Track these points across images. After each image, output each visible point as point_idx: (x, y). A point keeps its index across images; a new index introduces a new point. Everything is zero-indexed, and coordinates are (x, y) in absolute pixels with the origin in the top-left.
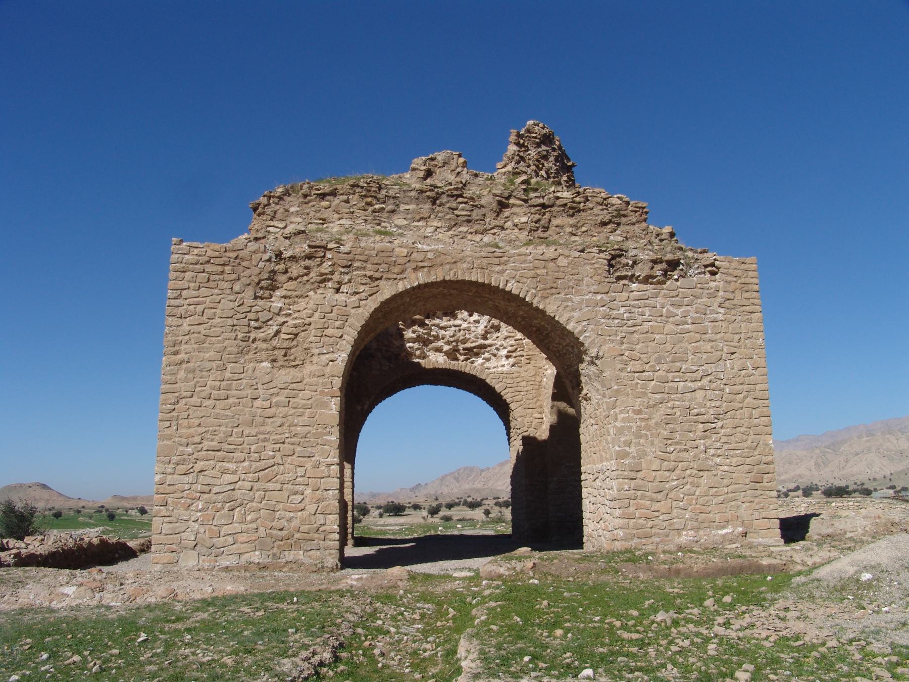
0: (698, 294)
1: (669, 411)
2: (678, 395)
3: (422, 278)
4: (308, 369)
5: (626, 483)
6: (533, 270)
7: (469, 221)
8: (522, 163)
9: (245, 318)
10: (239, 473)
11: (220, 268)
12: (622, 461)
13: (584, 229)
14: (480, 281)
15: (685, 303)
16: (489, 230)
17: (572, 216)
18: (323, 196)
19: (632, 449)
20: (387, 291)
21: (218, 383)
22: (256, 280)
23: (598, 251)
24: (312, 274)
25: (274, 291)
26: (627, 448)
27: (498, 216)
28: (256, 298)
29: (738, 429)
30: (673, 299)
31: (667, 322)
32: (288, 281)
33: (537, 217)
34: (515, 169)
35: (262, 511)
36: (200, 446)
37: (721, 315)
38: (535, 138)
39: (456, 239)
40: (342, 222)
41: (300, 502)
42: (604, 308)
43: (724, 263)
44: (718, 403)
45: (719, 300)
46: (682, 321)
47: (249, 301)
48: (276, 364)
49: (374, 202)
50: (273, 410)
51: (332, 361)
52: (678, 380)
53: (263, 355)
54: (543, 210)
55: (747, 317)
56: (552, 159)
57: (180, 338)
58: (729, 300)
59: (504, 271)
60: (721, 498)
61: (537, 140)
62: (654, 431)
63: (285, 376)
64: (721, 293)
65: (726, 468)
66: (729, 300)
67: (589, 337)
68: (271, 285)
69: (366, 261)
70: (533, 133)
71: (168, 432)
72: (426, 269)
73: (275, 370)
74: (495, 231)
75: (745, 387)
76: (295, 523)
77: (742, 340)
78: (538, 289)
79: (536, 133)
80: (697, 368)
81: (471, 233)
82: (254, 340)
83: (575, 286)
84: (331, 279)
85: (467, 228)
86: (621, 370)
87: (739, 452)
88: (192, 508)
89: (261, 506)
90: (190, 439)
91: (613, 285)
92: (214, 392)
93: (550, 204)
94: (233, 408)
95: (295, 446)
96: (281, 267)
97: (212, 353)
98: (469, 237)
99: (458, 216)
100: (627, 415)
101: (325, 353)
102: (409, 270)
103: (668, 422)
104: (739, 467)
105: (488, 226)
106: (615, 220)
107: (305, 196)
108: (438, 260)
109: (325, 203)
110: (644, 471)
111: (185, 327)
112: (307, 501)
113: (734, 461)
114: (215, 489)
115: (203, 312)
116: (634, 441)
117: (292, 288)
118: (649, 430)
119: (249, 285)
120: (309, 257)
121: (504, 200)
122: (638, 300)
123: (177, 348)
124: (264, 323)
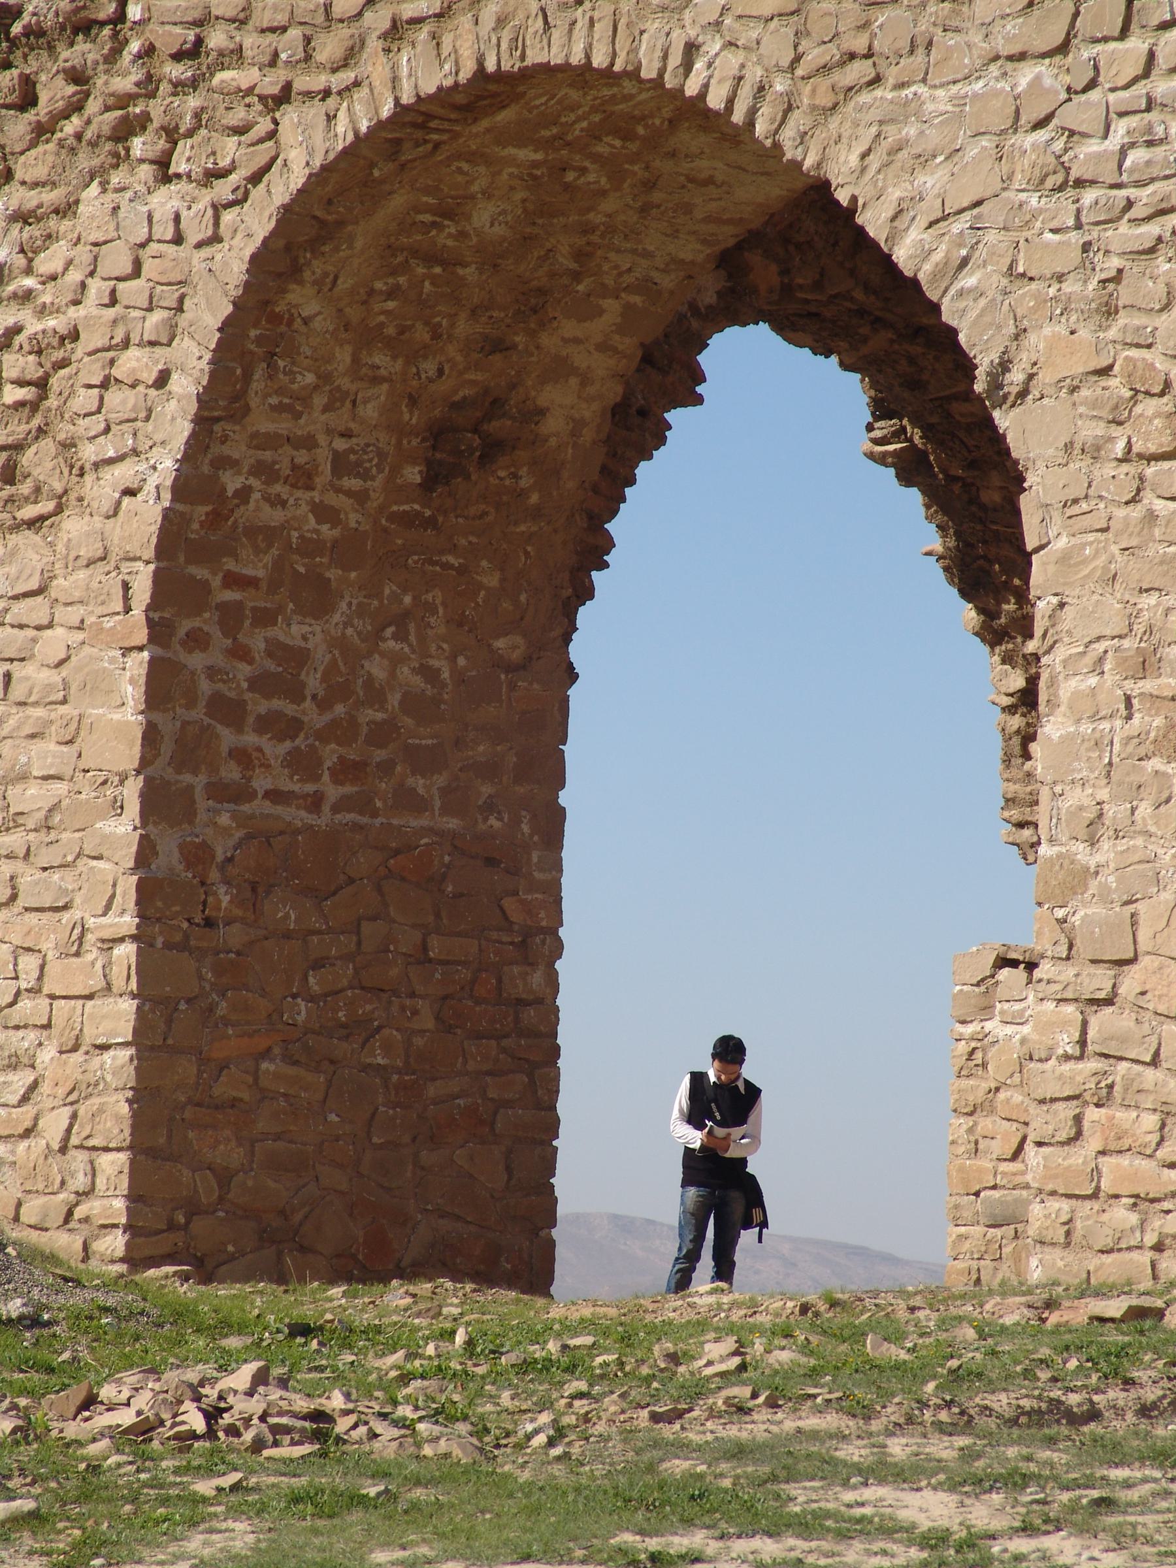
4: (73, 526)
5: (1064, 1024)
12: (1060, 913)
14: (599, 60)
19: (1107, 851)
24: (93, 106)
32: (33, 144)
41: (25, 1099)
42: (1042, 135)
51: (130, 492)
67: (978, 293)
72: (423, 34)
78: (799, 72)
86: (1095, 451)
95: (18, 866)
100: (1093, 681)
101: (111, 461)
102: (374, 44)
110: (1145, 961)
112: (45, 1088)
116: (1110, 811)
117: (40, 172)
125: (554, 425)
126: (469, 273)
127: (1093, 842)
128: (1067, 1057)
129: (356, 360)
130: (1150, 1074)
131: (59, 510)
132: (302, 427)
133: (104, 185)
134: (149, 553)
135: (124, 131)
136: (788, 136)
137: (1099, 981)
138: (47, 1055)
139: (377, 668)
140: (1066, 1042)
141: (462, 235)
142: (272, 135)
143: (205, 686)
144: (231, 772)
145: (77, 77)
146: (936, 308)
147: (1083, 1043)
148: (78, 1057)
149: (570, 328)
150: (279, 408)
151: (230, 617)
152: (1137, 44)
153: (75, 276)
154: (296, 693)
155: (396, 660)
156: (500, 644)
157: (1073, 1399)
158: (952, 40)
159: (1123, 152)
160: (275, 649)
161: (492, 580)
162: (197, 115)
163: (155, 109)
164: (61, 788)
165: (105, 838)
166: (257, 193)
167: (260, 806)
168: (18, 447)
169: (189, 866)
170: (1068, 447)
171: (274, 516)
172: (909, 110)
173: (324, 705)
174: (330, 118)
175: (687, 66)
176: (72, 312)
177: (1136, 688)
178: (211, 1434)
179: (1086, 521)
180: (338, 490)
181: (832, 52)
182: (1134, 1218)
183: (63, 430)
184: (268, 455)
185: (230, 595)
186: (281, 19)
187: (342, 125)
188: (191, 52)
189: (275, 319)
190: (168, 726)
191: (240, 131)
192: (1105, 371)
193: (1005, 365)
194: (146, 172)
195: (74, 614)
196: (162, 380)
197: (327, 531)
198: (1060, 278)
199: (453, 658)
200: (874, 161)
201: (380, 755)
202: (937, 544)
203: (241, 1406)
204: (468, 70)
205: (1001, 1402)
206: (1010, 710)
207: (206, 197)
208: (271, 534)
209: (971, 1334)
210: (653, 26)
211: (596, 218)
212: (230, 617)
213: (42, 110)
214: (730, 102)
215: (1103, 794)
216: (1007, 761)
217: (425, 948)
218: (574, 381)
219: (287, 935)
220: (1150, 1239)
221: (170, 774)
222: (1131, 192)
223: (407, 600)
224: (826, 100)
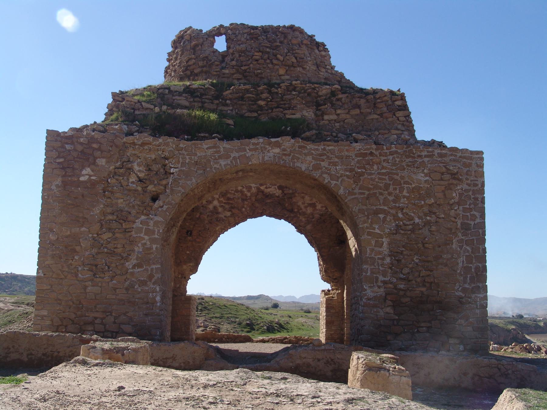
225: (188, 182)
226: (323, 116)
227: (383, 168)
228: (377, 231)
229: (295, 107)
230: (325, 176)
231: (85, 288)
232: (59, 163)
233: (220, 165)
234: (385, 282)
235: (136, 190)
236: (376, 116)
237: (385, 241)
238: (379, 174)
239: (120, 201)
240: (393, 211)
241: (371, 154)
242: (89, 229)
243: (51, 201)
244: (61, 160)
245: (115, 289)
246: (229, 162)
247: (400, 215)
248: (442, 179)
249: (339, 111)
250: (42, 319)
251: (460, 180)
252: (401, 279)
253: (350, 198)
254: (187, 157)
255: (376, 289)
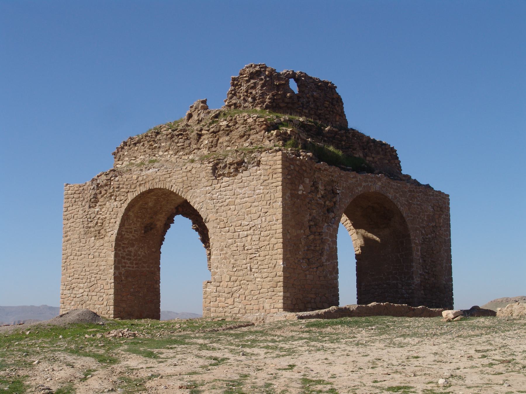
0: (251, 180)
1: (235, 249)
2: (239, 239)
3: (143, 189)
4: (106, 238)
5: (214, 289)
6: (182, 178)
7: (183, 148)
8: (235, 97)
9: (86, 217)
10: (84, 288)
11: (78, 195)
13: (233, 141)
14: (162, 187)
15: (245, 186)
16: (192, 151)
17: (228, 135)
18: (135, 144)
19: (218, 270)
20: (131, 197)
21: (78, 249)
22: (89, 199)
23: (207, 163)
24: (108, 193)
25: (97, 203)
26: (216, 270)
27: (198, 141)
28: (90, 207)
29: (267, 257)
30: (239, 184)
31: (237, 198)
32: (101, 198)
33: (211, 139)
34: (229, 103)
35: (91, 305)
36: (73, 277)
37: (262, 190)
38: (246, 77)
39: (178, 160)
40: (142, 157)
41: (102, 300)
42: (209, 194)
43: (265, 158)
44: (257, 242)
45: (261, 181)
46: (242, 197)
47: (87, 210)
48: (96, 238)
49: (153, 144)
50: (94, 259)
51: (112, 234)
52: (239, 231)
53: (93, 234)
54: (214, 135)
55: (274, 189)
56: (259, 87)
57: (67, 230)
58: (266, 180)
59: (171, 180)
60: (256, 297)
61: (247, 78)
62: (228, 260)
63: (98, 243)
64: (262, 176)
65: (259, 279)
66: (266, 180)
67: (203, 211)
68: (95, 200)
69: (123, 184)
70: (244, 74)
71: (65, 271)
72: (143, 185)
73: (96, 241)
74: (195, 151)
75: (272, 232)
76: (101, 310)
77: (271, 203)
79: (246, 74)
80: (248, 223)
81: (184, 155)
82: (90, 227)
83: (198, 184)
84: (113, 195)
85: (182, 152)
86: (216, 228)
87: (265, 270)
88: (71, 304)
89: (90, 303)
90: (70, 274)
91: (214, 181)
92: (78, 253)
93: (217, 130)
94: (83, 259)
95: (101, 275)
96: (98, 191)
97: (77, 235)
98: (183, 157)
99: (179, 146)
100: (217, 252)
102: (138, 186)
103: (234, 254)
104: (266, 279)
105: (192, 149)
106: (248, 133)
107: (129, 146)
108: (147, 180)
109: (136, 148)
110: (223, 282)
111: (69, 225)
112: (104, 299)
113: (265, 275)
114: (78, 296)
115: (74, 217)
117: (102, 201)
118: (226, 259)
119: (87, 202)
120: (106, 185)
121: (199, 133)
122: (225, 187)
123: (67, 234)
124: (93, 219)
125: (158, 226)
126: (149, 210)
127: (217, 269)
128: (215, 292)
129: (136, 220)
130: (224, 294)
131: (104, 237)
132: (131, 227)
133: (109, 202)
134: (114, 241)
135: (111, 196)
136: (182, 195)
137: (218, 284)
138: (104, 296)
139: (139, 253)
140: (215, 291)
141: (148, 206)
142: (127, 196)
143: (121, 255)
144: (124, 264)
145: (106, 190)
146: (199, 213)
147: (216, 291)
148: (108, 296)
149: (160, 216)
150: (128, 225)
151: (123, 248)
152: (219, 185)
153: (106, 212)
154: (131, 256)
155: (141, 252)
156: (153, 250)
157: (216, 329)
158: (199, 185)
159: (218, 196)
160: (128, 251)
161: (152, 243)
162: (119, 194)
163: (114, 194)
164: (105, 267)
165: (110, 272)
166: (125, 202)
167: (127, 268)
168: (100, 230)
169: (119, 275)
170: (213, 227)
171: (128, 237)
172: (195, 192)
173: (134, 257)
174: (133, 194)
175: (171, 188)
176: (106, 215)
177: (221, 253)
178: (123, 336)
179: (215, 235)
180: (135, 234)
181: (187, 186)
182: (222, 309)
183: (105, 228)
184: (127, 230)
185: (123, 245)
186: (128, 184)
187: (134, 195)
188: (118, 187)
189: (128, 215)
190: (117, 260)
191: (123, 196)
192: (217, 219)
193: (206, 219)
194: (113, 200)
195: (106, 248)
196: (115, 222)
197: (134, 238)
198: (212, 209)
199: (148, 251)
200: (192, 197)
201: (140, 262)
202: (200, 238)
203: (126, 333)
204: (148, 189)
205: (208, 329)
206: (208, 255)
207: (120, 203)
208: (127, 239)
209: (205, 322)
210: (168, 184)
211: (162, 204)
212: (123, 248)
213: (102, 194)
214: (176, 191)
215: (218, 264)
216: (208, 261)
217: (145, 283)
218: (160, 221)
219: (130, 282)
220: (224, 311)
221: (117, 265)
222: (219, 200)
223: (143, 245)
224: (186, 191)
225: (346, 201)
226: (366, 157)
227: (418, 201)
228: (417, 242)
229: (356, 149)
230: (398, 203)
231: (306, 275)
232: (288, 179)
233: (359, 191)
234: (421, 274)
235: (322, 204)
236: (387, 161)
237: (419, 247)
238: (417, 204)
239: (315, 211)
240: (421, 229)
241: (414, 191)
242: (304, 231)
243: (287, 208)
244: (289, 177)
245: (319, 277)
246: (362, 189)
247: (423, 232)
248: (437, 211)
249: (373, 155)
250: (287, 299)
251: (443, 212)
252: (426, 272)
253: (408, 219)
254: (345, 183)
255: (418, 279)
